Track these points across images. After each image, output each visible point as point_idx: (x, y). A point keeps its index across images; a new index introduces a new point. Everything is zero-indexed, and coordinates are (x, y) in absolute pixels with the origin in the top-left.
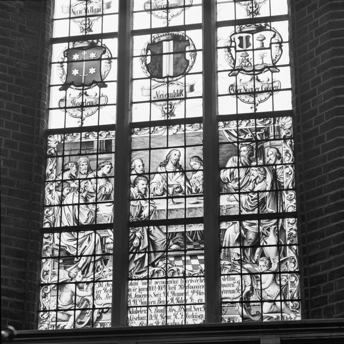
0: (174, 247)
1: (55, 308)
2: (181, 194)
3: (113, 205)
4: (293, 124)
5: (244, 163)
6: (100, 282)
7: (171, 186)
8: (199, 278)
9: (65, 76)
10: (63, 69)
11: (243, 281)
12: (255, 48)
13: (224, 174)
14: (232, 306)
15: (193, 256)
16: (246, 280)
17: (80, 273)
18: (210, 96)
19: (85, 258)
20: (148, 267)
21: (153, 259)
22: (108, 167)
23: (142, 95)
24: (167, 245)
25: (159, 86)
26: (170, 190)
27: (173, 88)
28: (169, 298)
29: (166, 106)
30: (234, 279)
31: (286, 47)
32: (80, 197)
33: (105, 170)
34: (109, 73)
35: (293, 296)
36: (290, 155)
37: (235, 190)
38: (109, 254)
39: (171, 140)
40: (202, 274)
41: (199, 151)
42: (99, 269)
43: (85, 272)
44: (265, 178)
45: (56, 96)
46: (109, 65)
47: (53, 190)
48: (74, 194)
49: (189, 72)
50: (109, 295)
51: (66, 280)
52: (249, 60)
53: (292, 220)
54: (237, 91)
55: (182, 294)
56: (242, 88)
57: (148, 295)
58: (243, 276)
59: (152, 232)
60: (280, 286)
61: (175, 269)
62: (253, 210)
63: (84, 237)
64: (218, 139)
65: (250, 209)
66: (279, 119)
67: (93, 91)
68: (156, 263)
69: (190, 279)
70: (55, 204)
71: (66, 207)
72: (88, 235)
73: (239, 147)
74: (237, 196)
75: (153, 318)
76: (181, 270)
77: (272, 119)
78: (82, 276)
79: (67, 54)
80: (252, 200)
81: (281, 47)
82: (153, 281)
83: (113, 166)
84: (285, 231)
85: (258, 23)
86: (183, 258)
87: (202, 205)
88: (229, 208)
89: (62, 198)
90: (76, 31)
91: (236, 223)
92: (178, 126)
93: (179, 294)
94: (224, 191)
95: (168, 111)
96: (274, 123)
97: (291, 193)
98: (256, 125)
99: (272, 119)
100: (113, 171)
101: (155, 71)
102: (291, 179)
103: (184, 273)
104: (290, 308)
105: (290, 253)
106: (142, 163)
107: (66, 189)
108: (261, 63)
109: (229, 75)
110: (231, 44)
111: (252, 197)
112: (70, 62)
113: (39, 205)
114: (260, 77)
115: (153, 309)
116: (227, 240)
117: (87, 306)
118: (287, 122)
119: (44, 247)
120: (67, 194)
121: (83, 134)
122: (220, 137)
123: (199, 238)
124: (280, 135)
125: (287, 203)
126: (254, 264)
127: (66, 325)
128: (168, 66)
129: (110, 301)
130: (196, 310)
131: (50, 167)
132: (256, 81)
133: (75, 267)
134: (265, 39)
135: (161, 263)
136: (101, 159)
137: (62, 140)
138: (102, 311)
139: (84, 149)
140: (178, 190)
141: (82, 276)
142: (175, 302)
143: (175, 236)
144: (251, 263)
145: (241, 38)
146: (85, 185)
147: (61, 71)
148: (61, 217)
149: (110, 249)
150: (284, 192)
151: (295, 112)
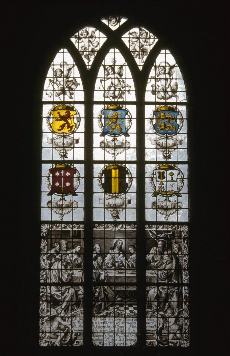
0: (119, 299)
1: (49, 331)
2: (123, 268)
4: (188, 230)
5: (160, 252)
6: (75, 317)
7: (117, 262)
8: (133, 318)
9: (50, 186)
10: (49, 181)
11: (158, 321)
12: (167, 180)
13: (149, 257)
14: (152, 335)
15: (130, 305)
16: (161, 321)
17: (63, 311)
18: (141, 208)
19: (66, 302)
21: (107, 306)
22: (79, 248)
24: (115, 297)
25: (110, 198)
26: (117, 264)
28: (116, 329)
29: (114, 212)
30: (153, 320)
31: (186, 181)
32: (62, 265)
33: (78, 249)
34: (78, 186)
36: (187, 249)
37: (155, 267)
38: (81, 301)
40: (135, 316)
41: (134, 241)
42: (75, 310)
43: (67, 311)
44: (172, 262)
45: (45, 199)
46: (78, 181)
47: (45, 259)
48: (58, 263)
49: (128, 191)
51: (55, 315)
53: (186, 288)
55: (124, 327)
57: (104, 326)
59: (106, 289)
60: (179, 325)
61: (119, 312)
62: (165, 280)
63: (65, 289)
66: (181, 226)
67: (69, 198)
68: (108, 308)
69: (128, 318)
70: (47, 268)
71: (54, 271)
73: (158, 241)
74: (156, 271)
75: (107, 340)
76: (123, 313)
77: (177, 226)
78: (64, 313)
81: (183, 181)
82: (107, 318)
84: (182, 294)
85: (169, 165)
86: (124, 306)
87: (135, 275)
88: (151, 277)
89: (51, 265)
90: (57, 158)
91: (154, 287)
92: (121, 225)
93: (122, 327)
95: (115, 215)
96: (178, 229)
97: (186, 272)
98: (167, 229)
99: (177, 226)
101: (107, 188)
102: (187, 263)
103: (125, 314)
104: (184, 338)
106: (100, 246)
107: (53, 259)
108: (171, 190)
109: (152, 195)
110: (154, 176)
111: (164, 272)
112: (54, 177)
113: (38, 268)
116: (150, 297)
117: (68, 331)
118: (185, 229)
119: (41, 294)
120: (54, 262)
121: (63, 225)
123: (134, 295)
124: (181, 236)
125: (184, 277)
127: (55, 342)
128: (115, 185)
129: (82, 329)
130: (131, 336)
131: (43, 244)
132: (168, 201)
133: (60, 308)
134: (173, 174)
135: (111, 308)
136: (74, 242)
137: (50, 228)
138: (77, 335)
140: (121, 265)
141: (64, 313)
142: (120, 331)
144: (163, 311)
145: (159, 173)
146: (65, 257)
147: (48, 183)
148: (51, 277)
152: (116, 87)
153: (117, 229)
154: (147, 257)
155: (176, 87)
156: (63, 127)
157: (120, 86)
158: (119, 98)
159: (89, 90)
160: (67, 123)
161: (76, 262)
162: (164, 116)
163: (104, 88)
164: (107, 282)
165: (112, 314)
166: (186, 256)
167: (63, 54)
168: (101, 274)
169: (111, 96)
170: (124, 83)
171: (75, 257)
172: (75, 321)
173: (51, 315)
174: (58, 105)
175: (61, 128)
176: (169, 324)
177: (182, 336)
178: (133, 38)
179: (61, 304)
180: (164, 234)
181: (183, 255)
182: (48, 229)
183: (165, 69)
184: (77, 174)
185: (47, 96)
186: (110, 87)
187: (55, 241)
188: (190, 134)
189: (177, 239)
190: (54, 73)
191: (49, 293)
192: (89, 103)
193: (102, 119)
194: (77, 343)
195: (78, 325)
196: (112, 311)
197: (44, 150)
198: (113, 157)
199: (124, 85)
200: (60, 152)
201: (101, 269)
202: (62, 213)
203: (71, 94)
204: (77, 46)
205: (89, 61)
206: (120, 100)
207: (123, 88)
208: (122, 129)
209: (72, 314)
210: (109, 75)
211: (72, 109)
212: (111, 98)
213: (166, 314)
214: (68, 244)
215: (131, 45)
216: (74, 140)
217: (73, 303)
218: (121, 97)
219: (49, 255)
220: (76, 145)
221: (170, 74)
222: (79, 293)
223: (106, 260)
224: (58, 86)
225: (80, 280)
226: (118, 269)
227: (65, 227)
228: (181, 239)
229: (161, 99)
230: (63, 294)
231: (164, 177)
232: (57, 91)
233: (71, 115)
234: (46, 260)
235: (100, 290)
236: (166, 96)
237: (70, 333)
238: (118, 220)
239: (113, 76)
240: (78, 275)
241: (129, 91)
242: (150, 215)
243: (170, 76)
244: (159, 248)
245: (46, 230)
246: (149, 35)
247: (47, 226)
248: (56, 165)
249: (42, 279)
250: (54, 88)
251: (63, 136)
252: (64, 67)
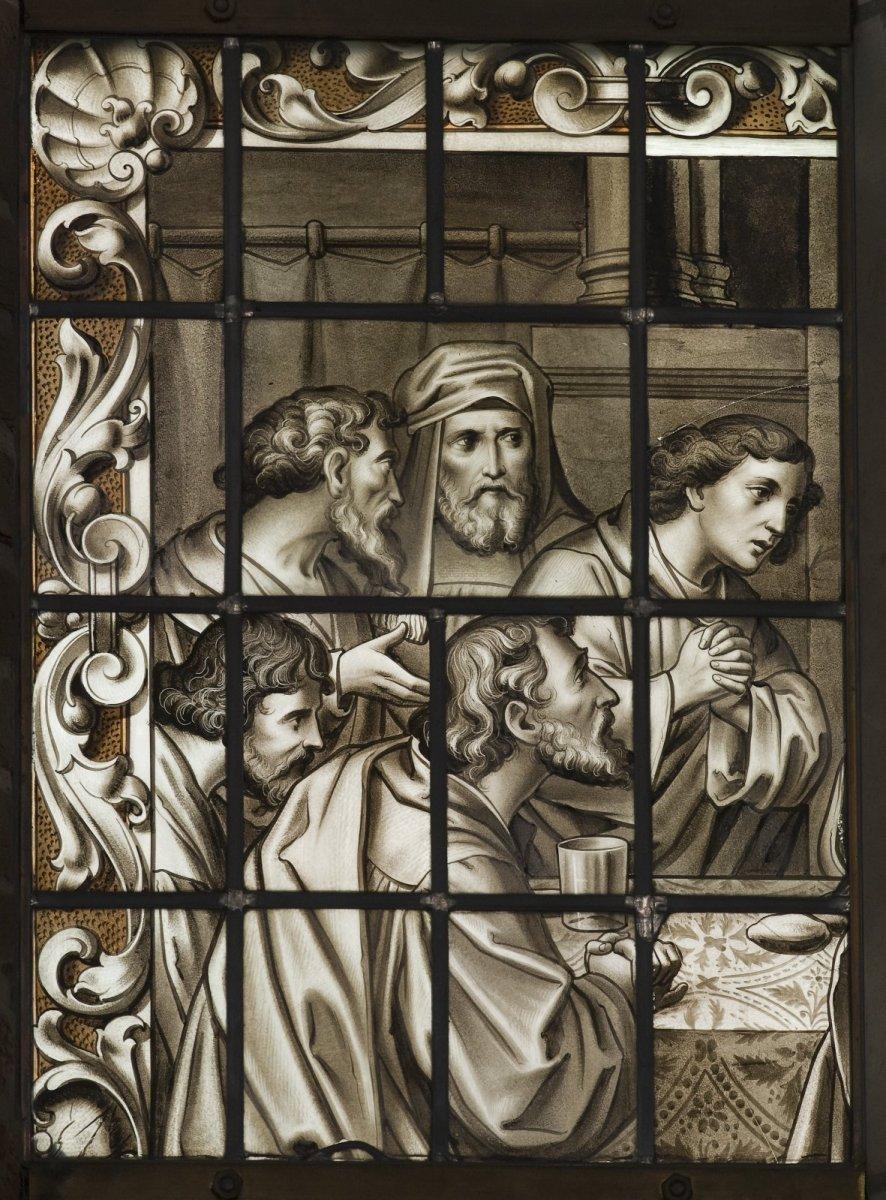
3: (837, 947)
22: (768, 489)
32: (455, 818)
33: (739, 515)
47: (126, 710)
48: (374, 776)
70: (163, 883)
71: (291, 924)
83: (825, 473)
89: (235, 815)
107: (282, 704)
120: (303, 765)
136: (682, 385)
137: (207, 113)
139: (481, 249)
146: (509, 676)
148: (233, 1038)
161: (719, 760)
171: (697, 661)
182: (166, 122)
214: (564, 414)
225: (794, 1109)
227: (499, 104)
234: (141, 720)
240: (757, 1020)
245: (129, 144)
247: (158, 76)
249: (76, 1091)
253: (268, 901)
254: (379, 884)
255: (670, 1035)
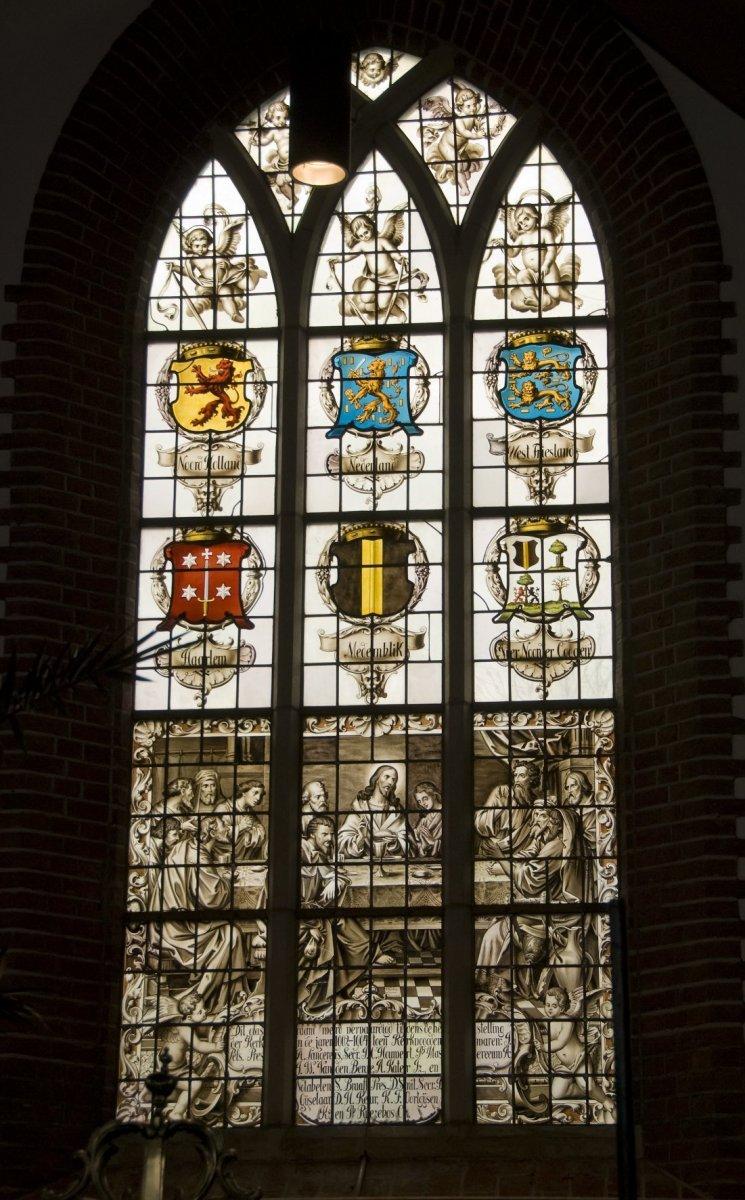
0: (384, 959)
3: (267, 871)
5: (521, 801)
6: (238, 1024)
7: (380, 839)
8: (430, 1024)
9: (167, 601)
10: (163, 585)
12: (545, 568)
13: (483, 819)
14: (494, 1083)
15: (422, 980)
17: (200, 1006)
19: (210, 975)
20: (333, 998)
21: (344, 983)
22: (257, 793)
23: (321, 648)
24: (372, 953)
25: (355, 633)
26: (378, 846)
27: (382, 640)
28: (374, 1062)
29: (369, 675)
31: (605, 569)
33: (252, 797)
35: (608, 1068)
37: (504, 853)
38: (257, 969)
39: (379, 747)
40: (438, 1017)
42: (238, 999)
44: (561, 832)
48: (188, 844)
49: (416, 609)
50: (257, 1052)
51: (174, 1019)
52: (534, 591)
54: (509, 652)
55: (400, 1055)
56: (520, 647)
58: (516, 1024)
59: (343, 927)
60: (586, 1046)
61: (384, 1002)
62: (537, 895)
64: (472, 748)
65: (531, 891)
67: (226, 634)
68: (349, 991)
70: (151, 864)
71: (173, 870)
72: (216, 928)
73: (513, 766)
74: (506, 864)
75: (344, 1100)
76: (398, 1005)
78: (204, 1011)
79: (171, 552)
80: (536, 874)
81: (596, 567)
82: (345, 1027)
83: (267, 789)
86: (402, 984)
87: (438, 881)
88: (491, 886)
89: (163, 852)
90: (188, 508)
93: (393, 1054)
94: (481, 853)
95: (372, 684)
96: (581, 722)
98: (546, 724)
100: (266, 800)
101: (346, 599)
103: (403, 1012)
104: (604, 1089)
105: (605, 982)
106: (324, 790)
107: (172, 832)
108: (557, 599)
109: (493, 620)
110: (499, 557)
111: (534, 868)
112: (179, 571)
113: (120, 864)
114: (556, 627)
115: (343, 1082)
117: (213, 1071)
118: (606, 722)
119: (129, 950)
120: (175, 843)
122: (476, 744)
123: (433, 945)
124: (590, 748)
125: (601, 882)
126: (537, 1000)
129: (259, 1063)
131: (139, 786)
132: (547, 634)
133: (191, 993)
134: (565, 549)
135: (359, 992)
136: (243, 775)
137: (163, 732)
140: (391, 848)
142: (386, 1069)
143: (387, 938)
145: (518, 545)
146: (211, 826)
147: (159, 590)
148: (162, 891)
149: (261, 959)
150: (597, 862)
151: (621, 701)
152: (380, 280)
153: (379, 732)
154: (477, 819)
155: (573, 269)
156: (209, 412)
157: (393, 277)
158: (390, 314)
159: (294, 291)
160: (224, 399)
161: (246, 839)
162: (535, 360)
163: (343, 288)
164: (347, 906)
165: (361, 1013)
166: (608, 812)
167: (213, 182)
168: (324, 880)
169: (365, 311)
170: (407, 265)
171: (244, 822)
172: (236, 1039)
173: (161, 1020)
174: (196, 345)
175: (203, 415)
176: (552, 1043)
177: (598, 1084)
178: (434, 119)
179: (195, 982)
180: (534, 742)
181: (597, 811)
183: (539, 214)
184: (251, 557)
185: (163, 314)
186: (361, 281)
187: (179, 773)
188: (621, 416)
189: (576, 756)
190: (183, 243)
191: (155, 946)
192: (293, 333)
193: (333, 383)
194: (241, 1113)
195: (248, 1053)
196: (362, 1001)
197: (148, 487)
198: (368, 500)
199: (404, 273)
200: (199, 493)
201: (326, 864)
202: (203, 685)
203: (237, 307)
204: (254, 153)
205: (294, 200)
206: (393, 320)
207: (402, 281)
208: (397, 413)
209: (229, 1012)
210: (358, 242)
211: (241, 356)
212: (365, 316)
213: (541, 1010)
214: (223, 781)
215: (429, 143)
216: (243, 451)
217: (235, 975)
218: (395, 309)
219: (158, 819)
220: (250, 469)
221: (552, 228)
222: (254, 943)
223: (344, 834)
224: (198, 284)
226: (381, 864)
227: (213, 728)
228: (590, 756)
229: (523, 310)
230: (199, 947)
231: (533, 560)
232: (194, 300)
233: (235, 374)
234: (148, 836)
235: (323, 933)
236: (539, 299)
237: (222, 1079)
238: (381, 701)
239: (369, 246)
240: (252, 884)
241: (421, 290)
242: (490, 683)
243: (554, 236)
244: (518, 789)
246: (483, 103)
247: (155, 726)
248: (184, 533)
249: (135, 900)
250: (182, 289)
251: (210, 442)
252: (214, 224)
253: (168, 866)
254: (188, 863)
255: (237, 888)
